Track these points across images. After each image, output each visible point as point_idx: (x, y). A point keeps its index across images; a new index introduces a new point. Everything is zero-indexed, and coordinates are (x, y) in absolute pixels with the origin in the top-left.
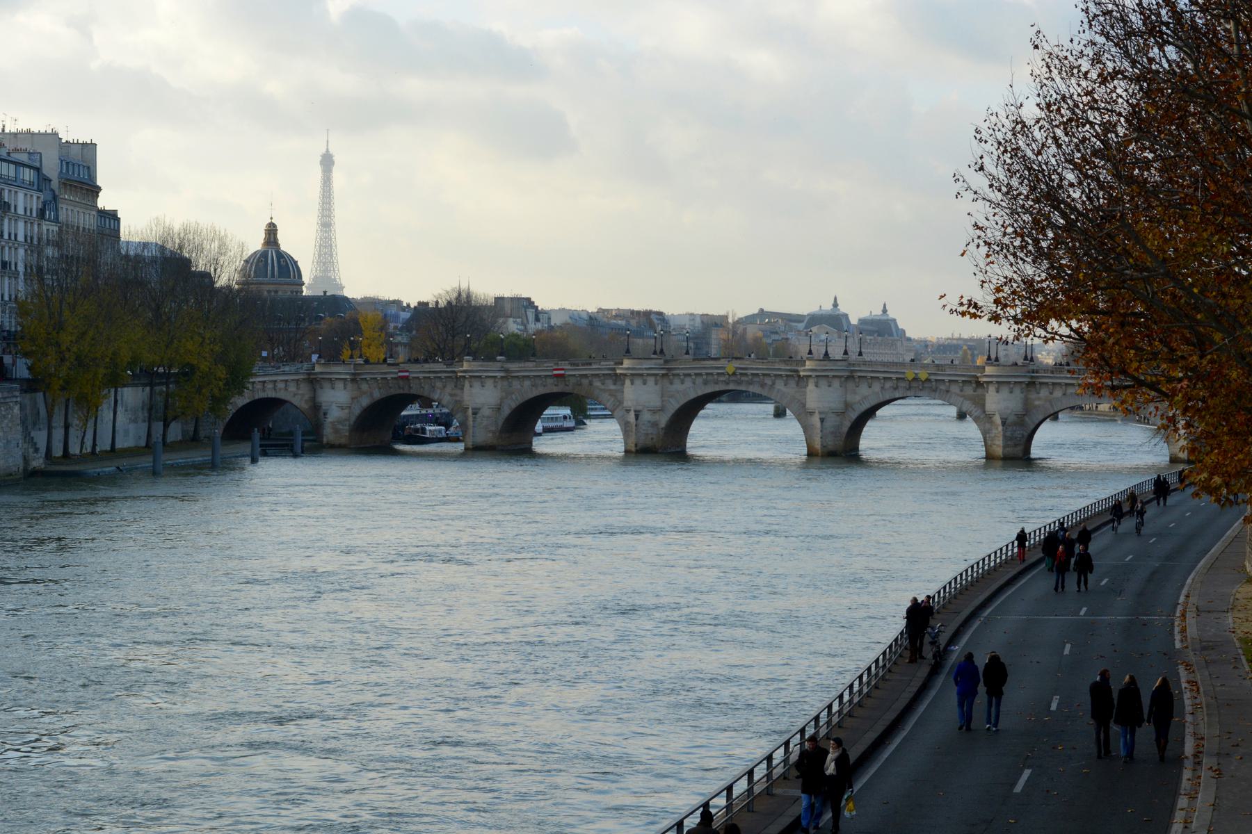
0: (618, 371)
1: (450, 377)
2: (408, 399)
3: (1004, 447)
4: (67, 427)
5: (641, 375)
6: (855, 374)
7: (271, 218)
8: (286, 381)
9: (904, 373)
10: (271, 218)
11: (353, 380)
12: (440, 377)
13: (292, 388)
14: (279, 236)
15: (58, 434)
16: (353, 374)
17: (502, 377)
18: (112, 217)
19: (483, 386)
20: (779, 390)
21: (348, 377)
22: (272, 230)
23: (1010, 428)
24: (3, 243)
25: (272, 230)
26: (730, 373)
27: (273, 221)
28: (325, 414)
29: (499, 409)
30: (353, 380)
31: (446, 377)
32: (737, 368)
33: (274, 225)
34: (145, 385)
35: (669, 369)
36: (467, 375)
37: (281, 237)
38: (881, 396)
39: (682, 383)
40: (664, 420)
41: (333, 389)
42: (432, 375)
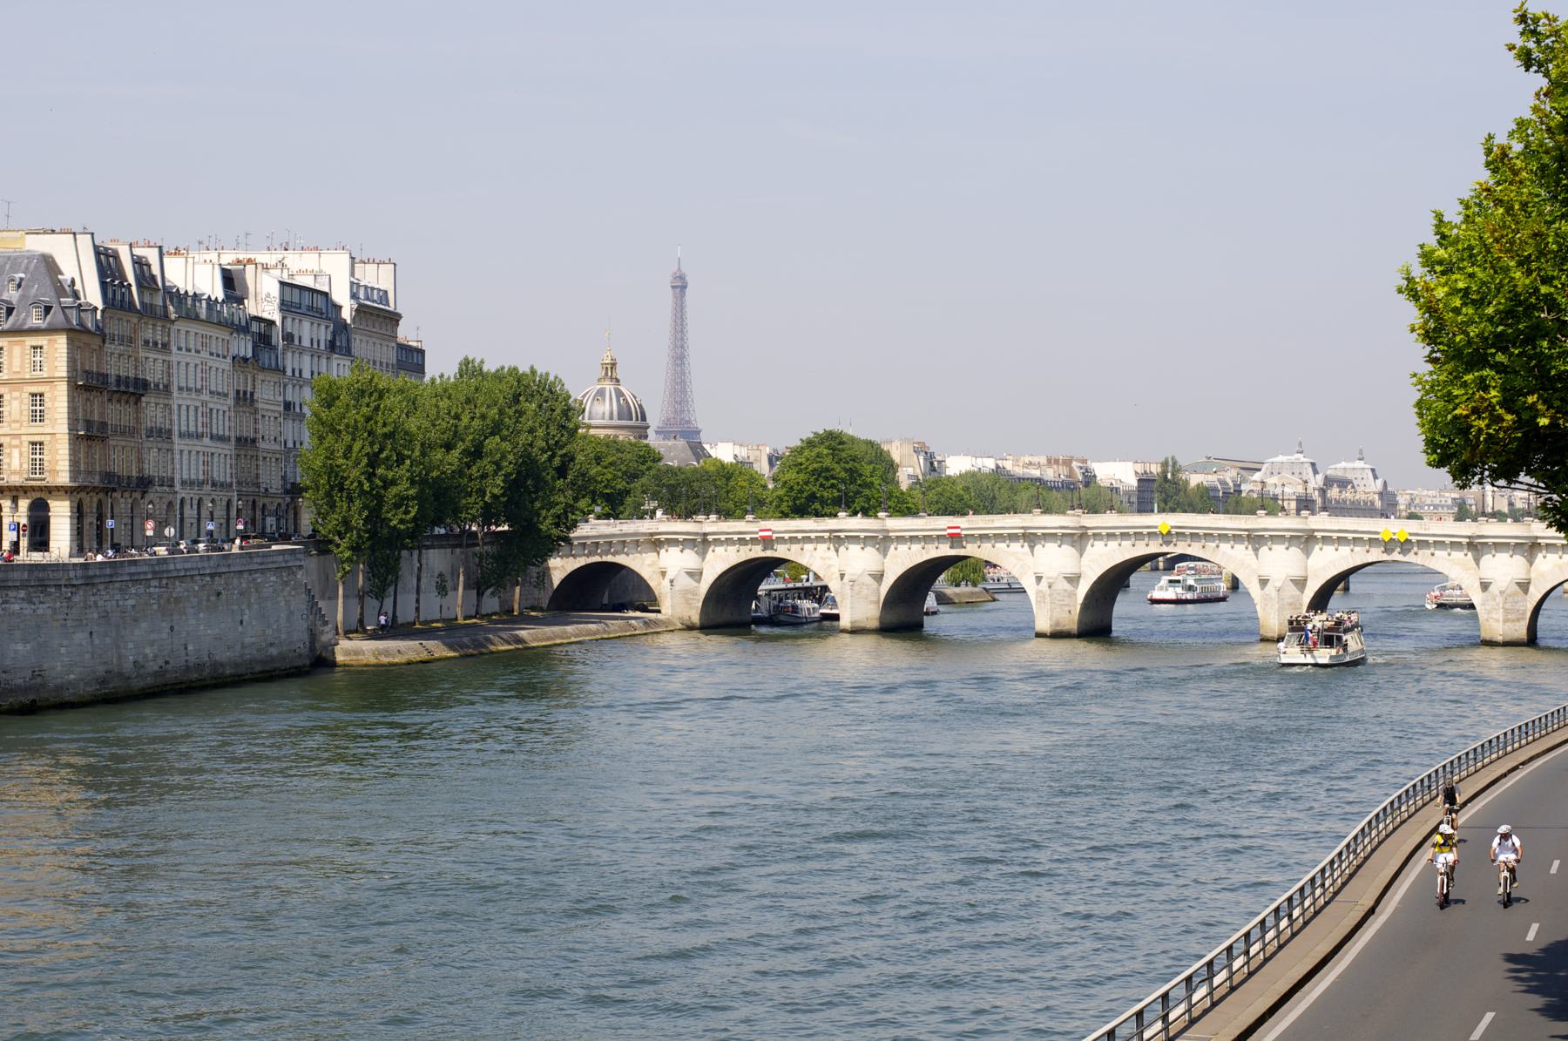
3: (1506, 621)
6: (1316, 534)
9: (1377, 533)
20: (1224, 553)
23: (1510, 599)
26: (1164, 533)
29: (879, 577)
32: (1172, 527)
34: (454, 546)
36: (842, 535)
38: (1350, 560)
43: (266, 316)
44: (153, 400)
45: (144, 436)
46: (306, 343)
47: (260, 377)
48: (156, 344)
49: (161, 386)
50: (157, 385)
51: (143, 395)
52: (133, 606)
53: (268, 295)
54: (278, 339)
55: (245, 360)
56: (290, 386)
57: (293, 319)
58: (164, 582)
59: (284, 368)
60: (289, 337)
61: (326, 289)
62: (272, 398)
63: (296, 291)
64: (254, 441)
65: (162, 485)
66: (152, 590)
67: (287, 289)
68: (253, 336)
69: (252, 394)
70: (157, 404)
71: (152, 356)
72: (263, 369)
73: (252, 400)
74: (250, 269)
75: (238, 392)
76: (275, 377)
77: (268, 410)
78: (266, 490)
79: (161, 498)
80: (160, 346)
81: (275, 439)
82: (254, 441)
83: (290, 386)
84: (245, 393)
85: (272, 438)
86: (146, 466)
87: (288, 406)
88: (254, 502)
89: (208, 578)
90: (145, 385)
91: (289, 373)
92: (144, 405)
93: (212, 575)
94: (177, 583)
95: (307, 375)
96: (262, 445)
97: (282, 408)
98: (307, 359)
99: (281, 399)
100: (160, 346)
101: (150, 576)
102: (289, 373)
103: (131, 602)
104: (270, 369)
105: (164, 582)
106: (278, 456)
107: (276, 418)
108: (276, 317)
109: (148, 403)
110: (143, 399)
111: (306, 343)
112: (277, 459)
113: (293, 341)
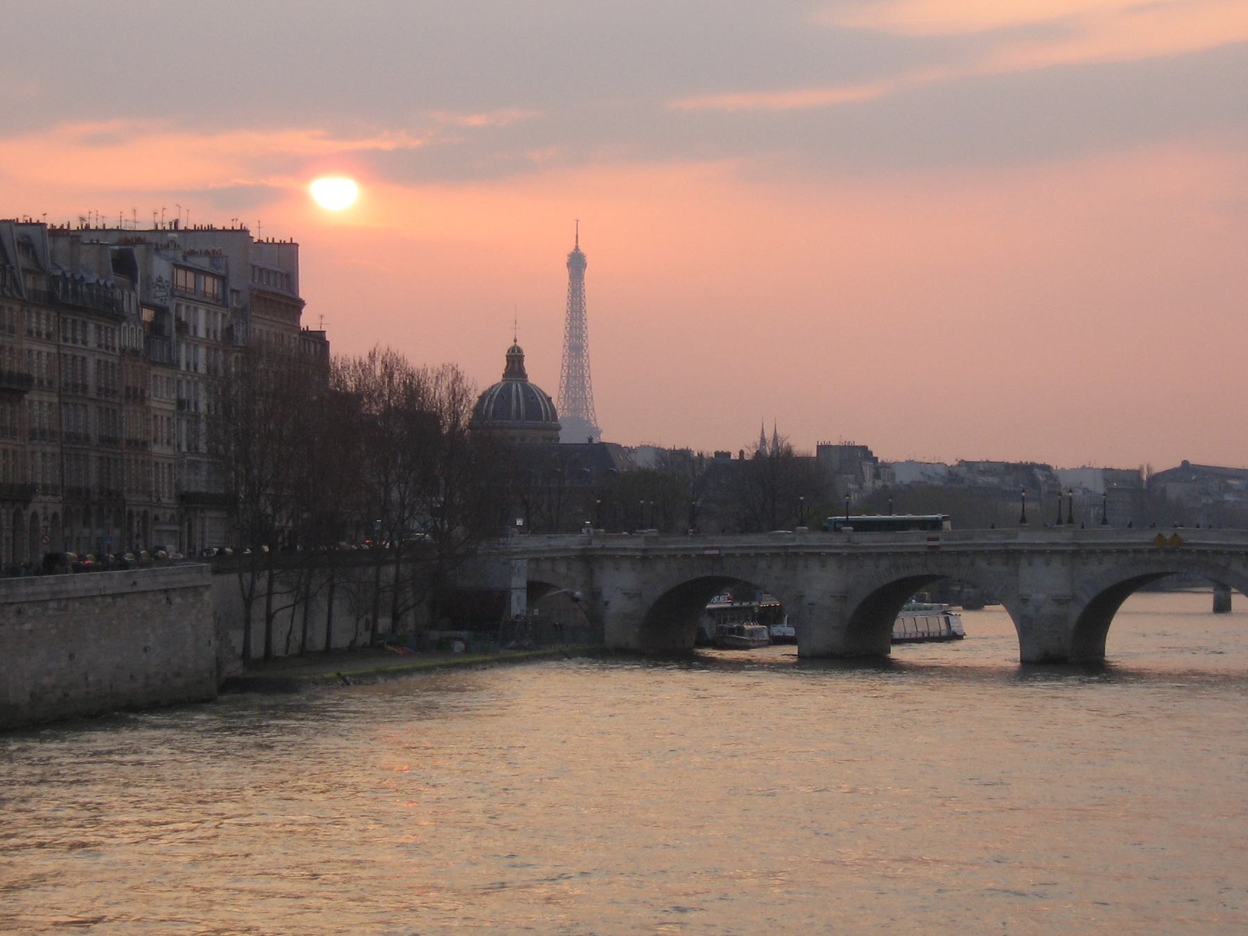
0: (1010, 547)
1: (778, 554)
2: (713, 586)
4: (269, 618)
5: (1043, 552)
7: (515, 341)
8: (553, 559)
10: (515, 341)
11: (644, 559)
12: (763, 555)
13: (562, 569)
14: (526, 364)
15: (258, 628)
16: (644, 550)
17: (849, 555)
18: (319, 340)
19: (823, 566)
21: (637, 554)
22: (515, 359)
24: (180, 376)
25: (515, 359)
27: (518, 344)
28: (607, 603)
29: (844, 597)
30: (644, 559)
31: (772, 554)
33: (519, 350)
35: (1079, 545)
37: (529, 365)
39: (1100, 564)
40: (1075, 613)
41: (617, 569)
42: (752, 552)
43: (157, 301)
44: (36, 398)
45: (27, 439)
46: (202, 333)
47: (154, 371)
48: (39, 334)
49: (45, 383)
50: (41, 382)
51: (26, 392)
52: (31, 631)
53: (160, 279)
54: (171, 326)
55: (135, 353)
56: (184, 383)
57: (188, 307)
58: (63, 603)
59: (178, 361)
60: (182, 327)
61: (222, 272)
62: (165, 395)
63: (191, 275)
64: (145, 444)
65: (45, 494)
66: (50, 612)
67: (181, 273)
68: (144, 326)
69: (143, 391)
70: (41, 403)
71: (35, 347)
72: (154, 363)
73: (143, 398)
74: (138, 251)
75: (128, 388)
76: (164, 373)
77: (160, 409)
78: (159, 500)
79: (45, 508)
80: (44, 337)
81: (168, 442)
82: (145, 444)
83: (184, 383)
84: (135, 390)
85: (165, 441)
86: (29, 472)
87: (181, 404)
88: (145, 512)
89: (109, 600)
90: (28, 380)
91: (183, 368)
92: (27, 403)
93: (114, 596)
94: (77, 604)
95: (202, 369)
96: (156, 449)
97: (173, 408)
98: (202, 352)
99: (174, 396)
100: (44, 337)
101: (47, 597)
102: (183, 368)
103: (28, 626)
104: (162, 364)
105: (63, 603)
106: (172, 462)
107: (169, 419)
108: (171, 304)
109: (31, 402)
110: (26, 396)
111: (202, 333)
112: (170, 465)
113: (187, 332)
